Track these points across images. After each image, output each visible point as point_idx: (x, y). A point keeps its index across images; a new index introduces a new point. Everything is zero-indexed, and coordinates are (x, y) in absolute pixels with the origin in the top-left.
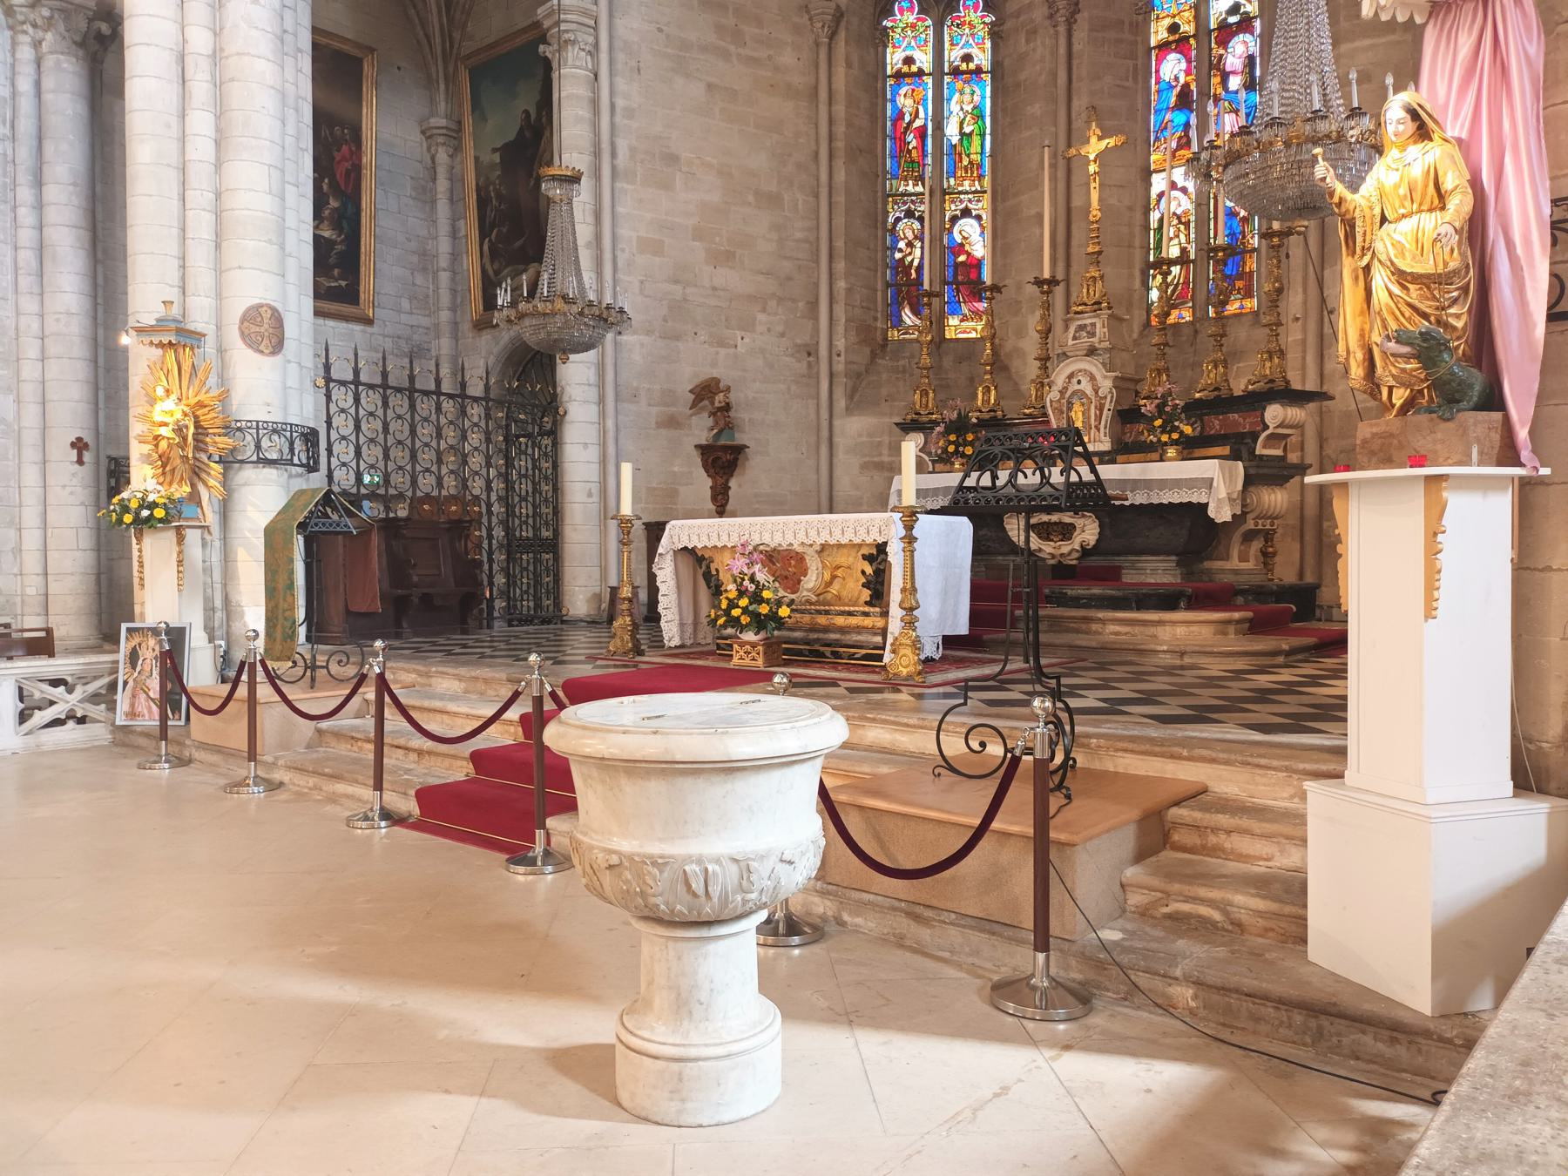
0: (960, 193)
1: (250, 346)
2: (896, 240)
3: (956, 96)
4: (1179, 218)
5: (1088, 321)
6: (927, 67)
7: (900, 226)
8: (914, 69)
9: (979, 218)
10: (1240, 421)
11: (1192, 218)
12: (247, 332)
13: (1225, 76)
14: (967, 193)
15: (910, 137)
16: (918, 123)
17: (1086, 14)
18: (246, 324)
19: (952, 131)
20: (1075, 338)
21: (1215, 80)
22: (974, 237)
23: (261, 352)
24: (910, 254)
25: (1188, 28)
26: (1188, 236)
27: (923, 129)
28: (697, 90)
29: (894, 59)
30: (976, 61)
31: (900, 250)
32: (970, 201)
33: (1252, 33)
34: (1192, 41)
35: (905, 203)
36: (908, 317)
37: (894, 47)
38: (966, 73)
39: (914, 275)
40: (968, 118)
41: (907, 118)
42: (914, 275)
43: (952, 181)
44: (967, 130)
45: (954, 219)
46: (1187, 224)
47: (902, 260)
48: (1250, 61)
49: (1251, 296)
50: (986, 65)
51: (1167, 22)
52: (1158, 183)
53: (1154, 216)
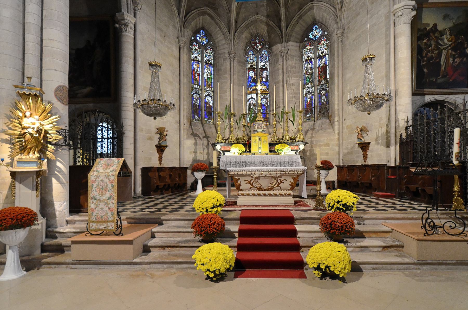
0: (207, 90)
1: (59, 101)
2: (193, 98)
3: (206, 68)
4: (253, 104)
5: (260, 124)
6: (200, 60)
7: (194, 95)
8: (197, 59)
9: (211, 97)
11: (256, 105)
12: (58, 95)
14: (209, 91)
15: (196, 75)
16: (198, 72)
17: (237, 58)
18: (57, 91)
19: (205, 75)
20: (257, 127)
23: (63, 103)
24: (197, 102)
25: (255, 67)
26: (255, 108)
27: (199, 74)
29: (193, 56)
30: (210, 62)
31: (194, 101)
32: (209, 93)
33: (267, 71)
34: (255, 70)
35: (195, 90)
37: (193, 53)
38: (207, 63)
39: (197, 108)
40: (209, 74)
41: (196, 71)
42: (197, 108)
43: (205, 87)
44: (209, 76)
45: (206, 96)
46: (255, 106)
47: (195, 103)
48: (267, 76)
49: (268, 122)
50: (213, 63)
51: (250, 64)
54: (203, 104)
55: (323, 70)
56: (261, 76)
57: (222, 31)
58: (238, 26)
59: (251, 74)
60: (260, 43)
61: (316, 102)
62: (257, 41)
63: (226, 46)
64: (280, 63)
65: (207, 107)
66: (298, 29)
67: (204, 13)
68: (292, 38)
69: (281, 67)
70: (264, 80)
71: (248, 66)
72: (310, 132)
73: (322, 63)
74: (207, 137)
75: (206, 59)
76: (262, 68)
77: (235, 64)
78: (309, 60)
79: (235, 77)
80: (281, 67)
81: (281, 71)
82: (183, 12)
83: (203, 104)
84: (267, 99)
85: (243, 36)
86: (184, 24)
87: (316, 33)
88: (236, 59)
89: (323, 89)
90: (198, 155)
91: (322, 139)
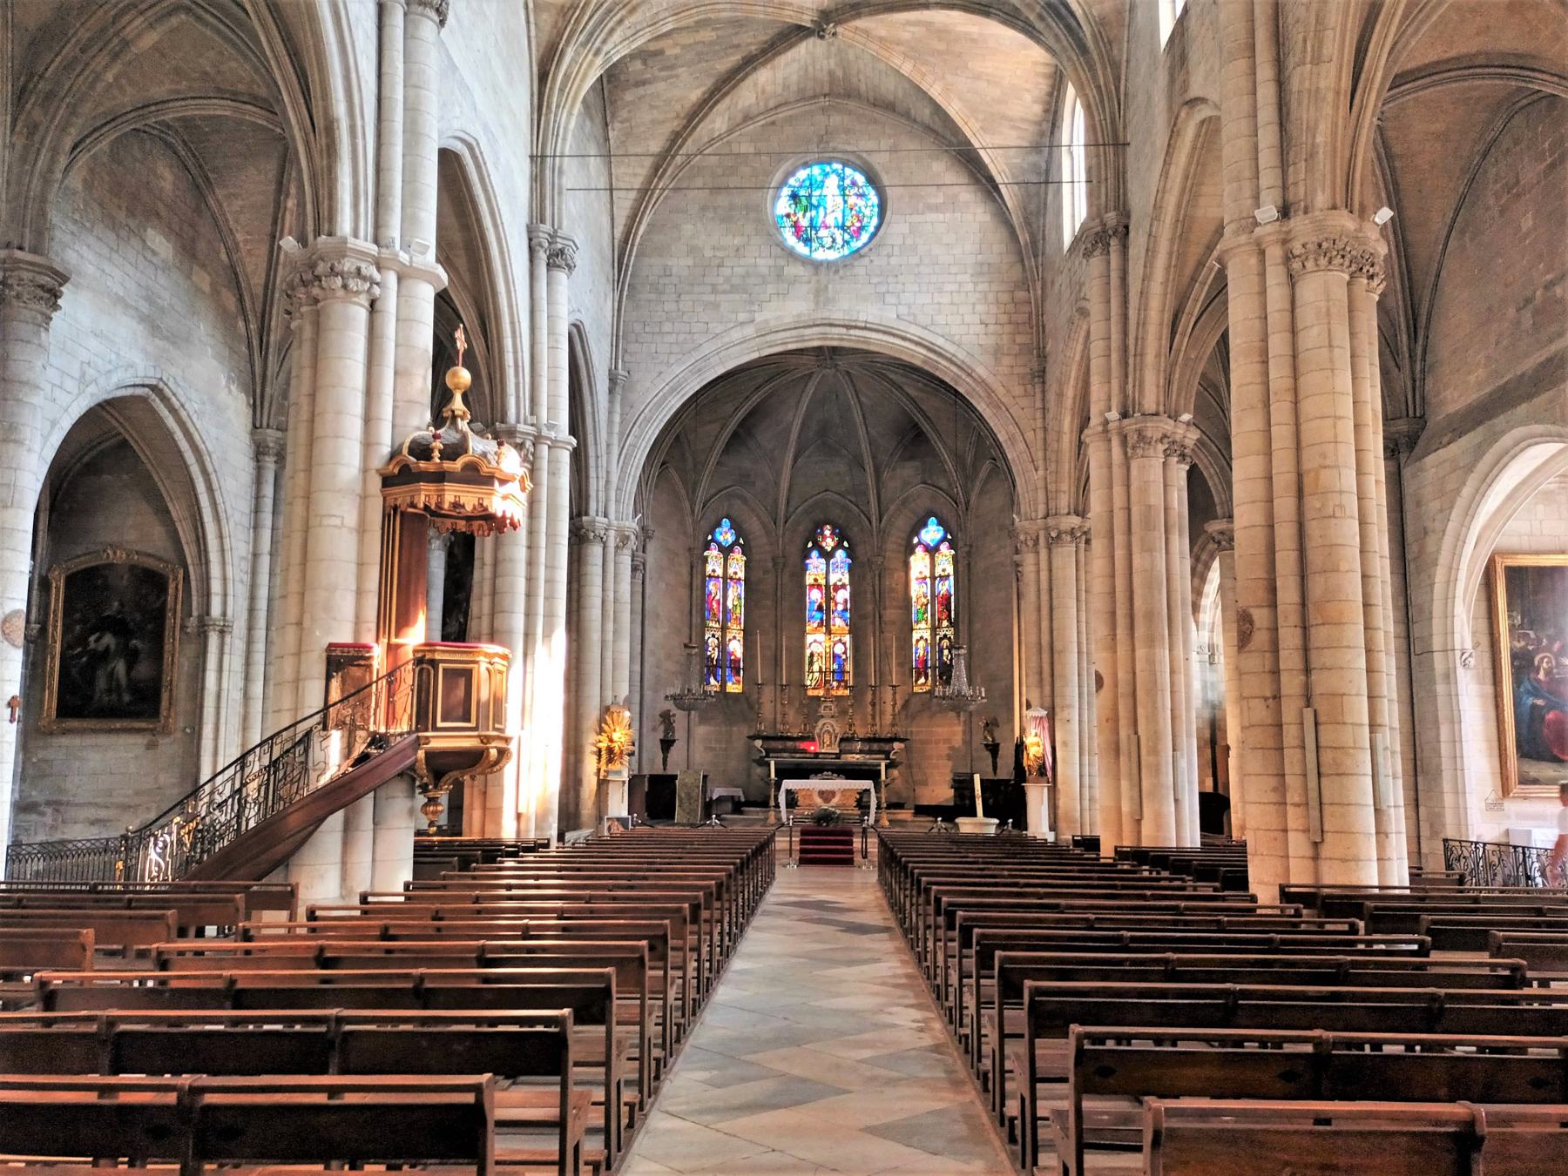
10: (887, 747)
13: (836, 604)
15: (714, 603)
19: (730, 604)
21: (832, 604)
22: (736, 648)
25: (823, 582)
28: (663, 585)
29: (709, 569)
36: (712, 681)
52: (809, 639)
53: (808, 653)
58: (791, 509)
62: (827, 533)
67: (730, 496)
70: (840, 608)
76: (835, 585)
84: (844, 644)
85: (801, 528)
88: (787, 571)
89: (945, 636)
91: (940, 730)
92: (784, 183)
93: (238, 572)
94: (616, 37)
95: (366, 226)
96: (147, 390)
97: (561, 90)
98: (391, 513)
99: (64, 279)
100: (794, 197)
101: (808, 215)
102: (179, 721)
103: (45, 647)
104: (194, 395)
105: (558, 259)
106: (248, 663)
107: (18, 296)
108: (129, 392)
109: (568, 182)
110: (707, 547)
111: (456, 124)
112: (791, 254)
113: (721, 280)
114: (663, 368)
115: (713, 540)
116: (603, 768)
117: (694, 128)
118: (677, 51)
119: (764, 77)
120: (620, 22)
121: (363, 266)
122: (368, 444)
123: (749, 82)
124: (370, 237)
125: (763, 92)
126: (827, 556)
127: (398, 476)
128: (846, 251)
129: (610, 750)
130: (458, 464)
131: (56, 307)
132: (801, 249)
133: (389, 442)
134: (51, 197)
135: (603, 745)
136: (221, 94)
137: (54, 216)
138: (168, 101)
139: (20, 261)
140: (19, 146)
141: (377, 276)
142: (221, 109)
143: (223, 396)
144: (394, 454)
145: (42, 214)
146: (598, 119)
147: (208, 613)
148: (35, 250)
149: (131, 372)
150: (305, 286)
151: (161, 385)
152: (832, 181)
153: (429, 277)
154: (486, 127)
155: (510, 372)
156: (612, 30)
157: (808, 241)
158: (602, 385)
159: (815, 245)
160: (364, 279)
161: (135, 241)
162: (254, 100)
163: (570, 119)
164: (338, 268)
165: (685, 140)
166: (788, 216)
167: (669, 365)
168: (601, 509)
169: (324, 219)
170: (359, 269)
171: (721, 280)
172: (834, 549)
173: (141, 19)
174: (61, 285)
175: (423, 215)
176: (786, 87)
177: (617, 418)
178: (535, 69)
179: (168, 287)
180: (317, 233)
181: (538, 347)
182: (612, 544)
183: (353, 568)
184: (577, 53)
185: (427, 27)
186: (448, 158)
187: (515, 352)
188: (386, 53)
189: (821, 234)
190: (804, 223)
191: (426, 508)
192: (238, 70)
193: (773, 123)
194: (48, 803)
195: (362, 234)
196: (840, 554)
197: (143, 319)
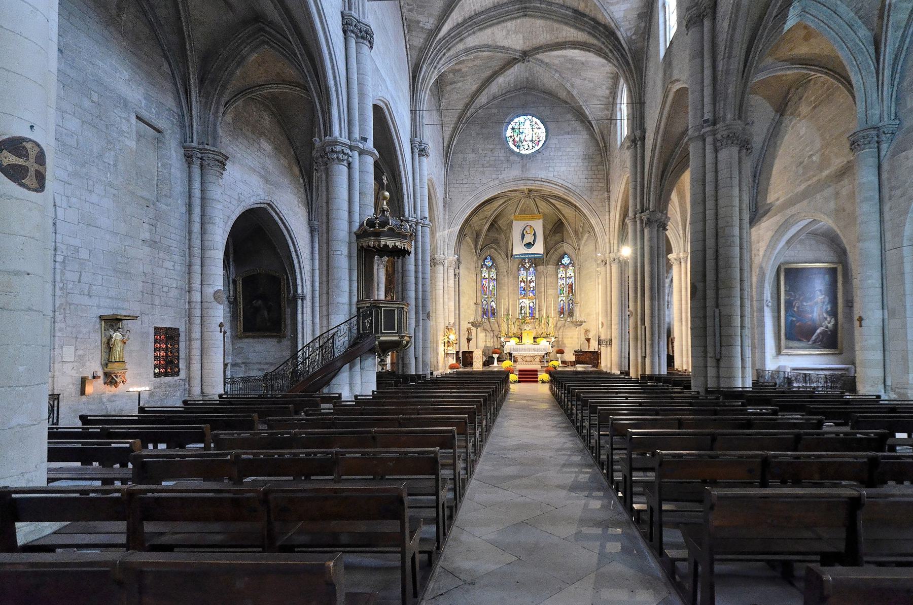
29: (483, 275)
54: (489, 308)
55: (571, 286)
56: (529, 286)
57: (502, 258)
59: (522, 284)
60: (528, 262)
61: (566, 308)
62: (527, 261)
63: (505, 267)
64: (543, 279)
65: (492, 310)
66: (555, 257)
67: (491, 248)
68: (551, 263)
69: (543, 282)
70: (532, 289)
71: (520, 279)
72: (562, 328)
73: (570, 281)
74: (493, 331)
75: (491, 276)
77: (511, 279)
78: (562, 278)
79: (511, 288)
80: (543, 282)
81: (543, 285)
82: (478, 251)
83: (489, 308)
86: (478, 258)
87: (566, 261)
90: (487, 343)
92: (509, 123)
93: (307, 276)
94: (442, 62)
95: (345, 133)
96: (266, 205)
97: (422, 83)
98: (361, 249)
99: (227, 158)
100: (513, 129)
101: (519, 136)
102: (289, 332)
103: (237, 305)
104: (284, 207)
105: (423, 152)
106: (313, 311)
107: (209, 164)
108: (258, 206)
109: (426, 121)
110: (482, 268)
111: (380, 94)
112: (512, 152)
113: (485, 162)
114: (464, 197)
115: (485, 264)
116: (446, 349)
117: (474, 101)
118: (467, 69)
119: (501, 80)
120: (444, 55)
121: (344, 149)
122: (350, 222)
123: (494, 83)
124: (347, 138)
125: (501, 86)
126: (527, 269)
127: (361, 234)
128: (534, 150)
129: (448, 342)
130: (386, 229)
131: (224, 169)
132: (516, 149)
133: (358, 221)
134: (218, 123)
135: (446, 340)
136: (284, 82)
137: (220, 132)
138: (263, 85)
139: (207, 150)
140: (203, 103)
141: (350, 153)
142: (285, 89)
143: (296, 208)
144: (361, 225)
145: (215, 130)
146: (437, 98)
147: (297, 292)
148: (214, 146)
149: (259, 197)
150: (322, 158)
151: (271, 203)
152: (528, 122)
153: (370, 153)
154: (392, 97)
155: (406, 197)
156: (441, 58)
157: (518, 147)
158: (441, 204)
159: (522, 148)
160: (345, 154)
161: (256, 144)
162: (297, 85)
163: (426, 96)
164: (334, 149)
165: (471, 106)
166: (511, 137)
167: (466, 196)
168: (442, 252)
169: (328, 130)
170: (343, 150)
171: (485, 162)
172: (529, 267)
173: (248, 47)
174: (226, 160)
175: (368, 128)
176: (509, 84)
177: (447, 217)
178: (411, 75)
179: (270, 164)
180: (325, 135)
181: (416, 187)
182: (446, 265)
183: (347, 271)
184: (427, 68)
185: (365, 48)
186: (376, 107)
187: (407, 189)
188: (349, 60)
189: (523, 144)
190: (517, 139)
191: (374, 247)
192: (290, 72)
193: (505, 100)
194: (243, 363)
195: (343, 136)
196: (532, 269)
197: (262, 177)
